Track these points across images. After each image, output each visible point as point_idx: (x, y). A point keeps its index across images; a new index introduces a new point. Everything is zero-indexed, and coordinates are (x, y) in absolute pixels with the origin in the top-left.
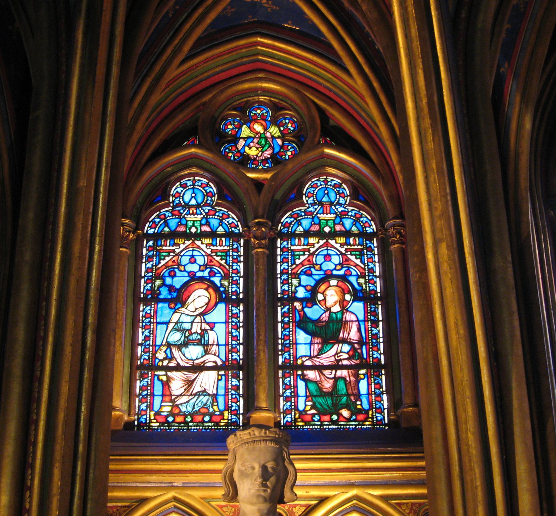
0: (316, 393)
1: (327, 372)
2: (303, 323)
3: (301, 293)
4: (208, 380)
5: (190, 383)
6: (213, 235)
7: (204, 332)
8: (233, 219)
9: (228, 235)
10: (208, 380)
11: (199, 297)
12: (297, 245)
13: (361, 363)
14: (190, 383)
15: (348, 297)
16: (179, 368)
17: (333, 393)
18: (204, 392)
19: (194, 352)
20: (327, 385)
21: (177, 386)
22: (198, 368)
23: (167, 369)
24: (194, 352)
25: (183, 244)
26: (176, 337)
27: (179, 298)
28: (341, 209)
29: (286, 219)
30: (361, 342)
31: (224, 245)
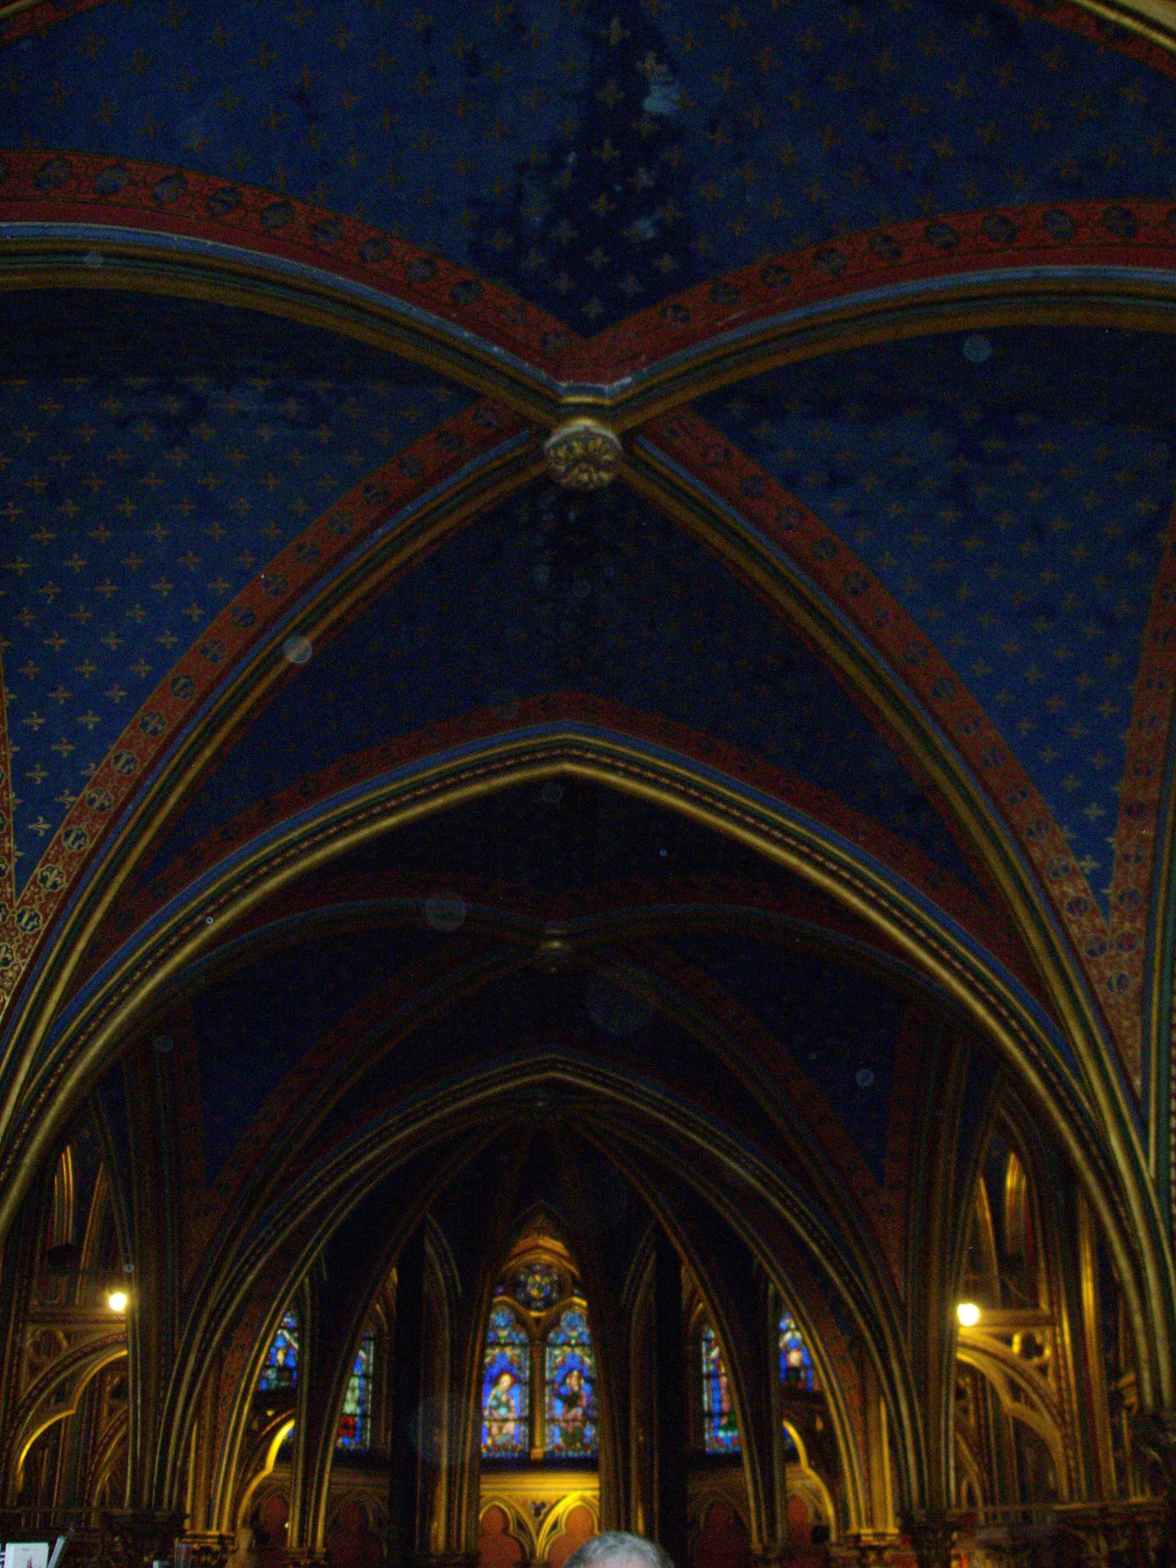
0: (565, 1434)
1: (571, 1424)
2: (558, 1395)
3: (559, 1379)
4: (510, 1427)
5: (500, 1429)
6: (512, 1344)
7: (508, 1401)
8: (523, 1335)
9: (523, 1345)
10: (510, 1427)
11: (506, 1380)
12: (557, 1352)
13: (587, 1418)
14: (500, 1429)
15: (582, 1382)
16: (495, 1420)
17: (573, 1435)
18: (508, 1434)
19: (503, 1411)
20: (570, 1430)
21: (495, 1430)
22: (506, 1420)
23: (490, 1421)
24: (503, 1411)
25: (497, 1351)
26: (494, 1403)
27: (495, 1381)
28: (580, 1329)
29: (552, 1335)
30: (588, 1406)
31: (517, 1351)
